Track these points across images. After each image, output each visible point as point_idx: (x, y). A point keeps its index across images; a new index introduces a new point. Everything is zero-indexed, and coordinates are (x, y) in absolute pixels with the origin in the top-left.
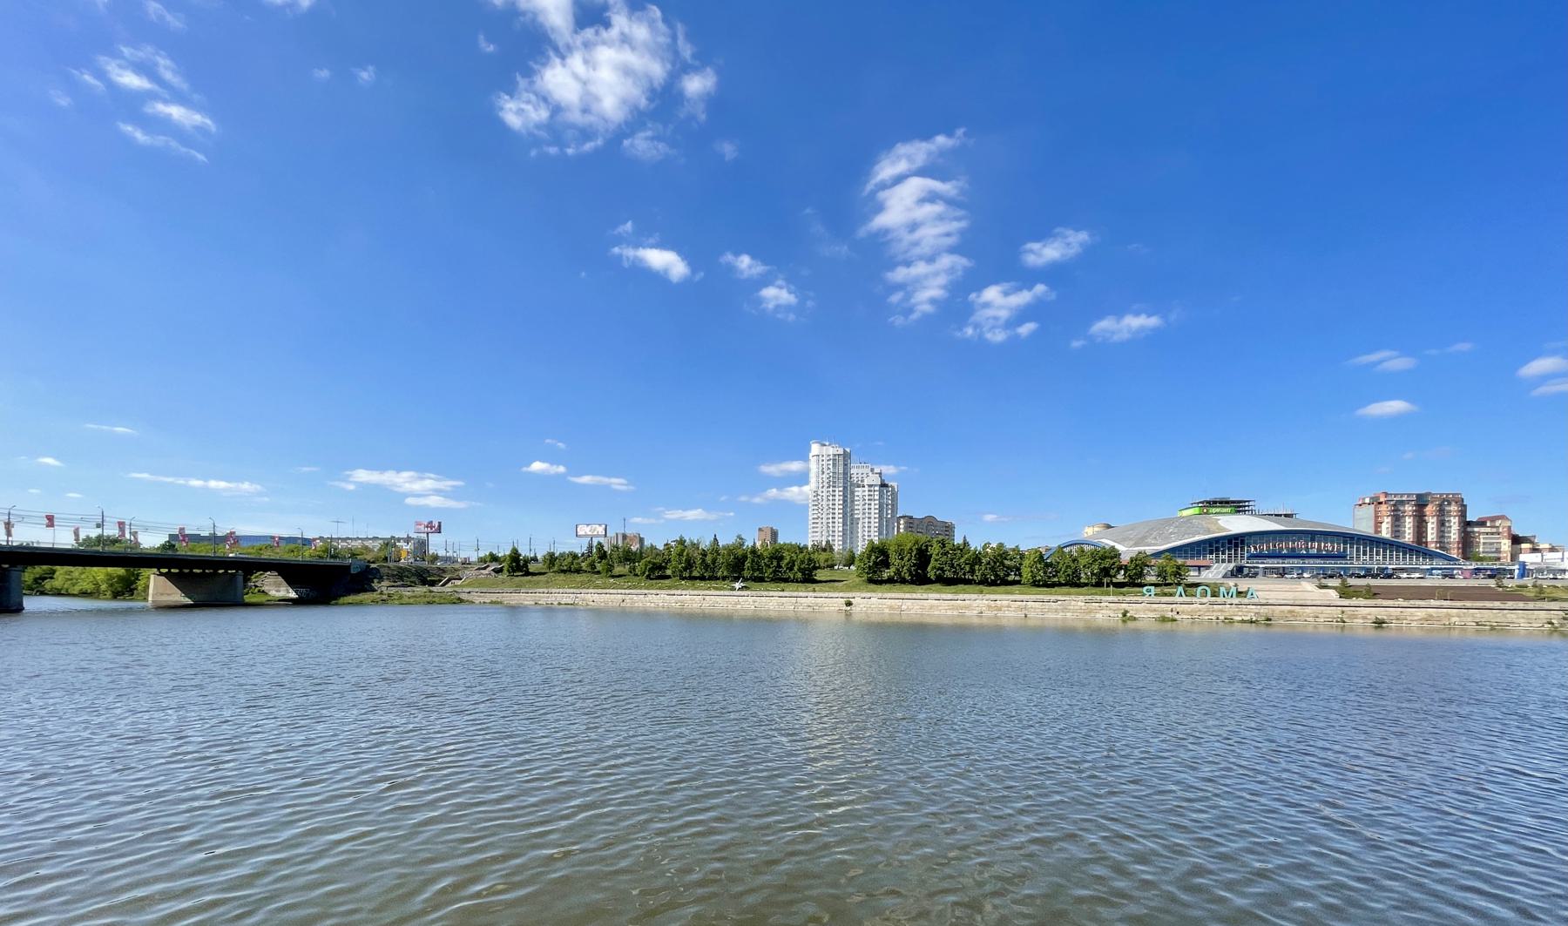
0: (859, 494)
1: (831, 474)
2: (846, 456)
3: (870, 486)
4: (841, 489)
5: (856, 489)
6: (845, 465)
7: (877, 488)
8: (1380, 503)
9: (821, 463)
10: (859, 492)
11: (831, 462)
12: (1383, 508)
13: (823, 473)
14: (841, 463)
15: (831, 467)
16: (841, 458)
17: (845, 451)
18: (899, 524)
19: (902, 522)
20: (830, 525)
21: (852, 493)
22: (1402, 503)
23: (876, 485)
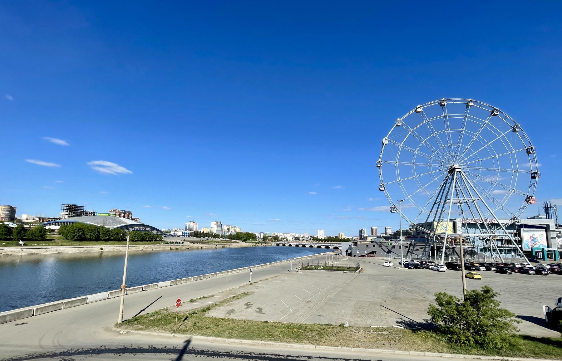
8: (117, 212)
12: (117, 213)
22: (121, 213)
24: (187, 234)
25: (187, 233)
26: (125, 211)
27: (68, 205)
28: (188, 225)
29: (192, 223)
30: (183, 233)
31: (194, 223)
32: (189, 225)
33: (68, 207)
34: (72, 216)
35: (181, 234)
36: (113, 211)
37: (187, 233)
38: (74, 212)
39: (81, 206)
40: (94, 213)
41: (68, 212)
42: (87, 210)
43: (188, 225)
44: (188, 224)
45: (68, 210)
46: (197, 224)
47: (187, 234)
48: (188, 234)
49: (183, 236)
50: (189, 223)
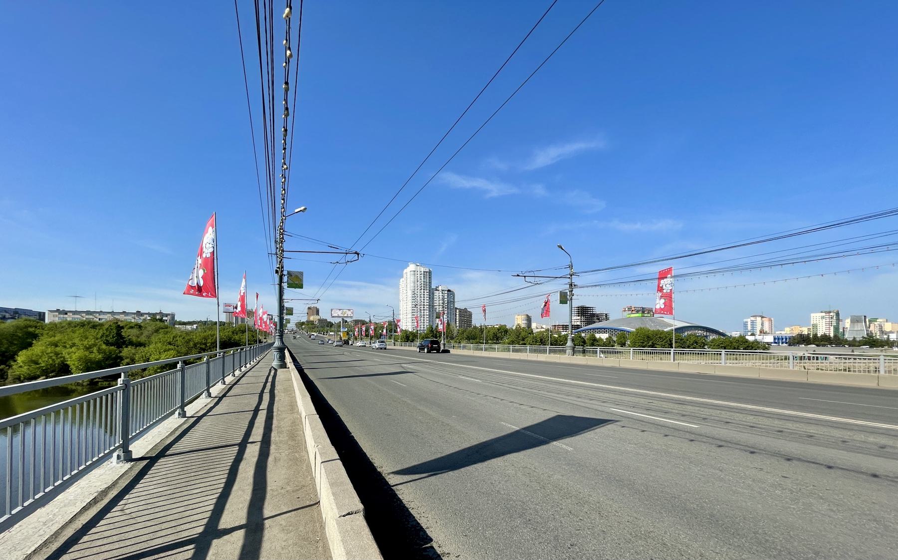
0: (437, 294)
1: (422, 282)
2: (430, 272)
3: (443, 290)
4: (428, 291)
5: (435, 292)
6: (430, 278)
7: (446, 292)
9: (416, 276)
10: (436, 293)
11: (422, 275)
13: (418, 281)
14: (428, 276)
15: (422, 278)
16: (428, 274)
17: (429, 270)
18: (456, 311)
19: (458, 311)
20: (422, 311)
21: (433, 294)
23: (445, 291)
24: (784, 340)
25: (779, 339)
26: (643, 308)
27: (578, 308)
28: (749, 324)
29: (759, 319)
30: (775, 339)
31: (764, 319)
32: (753, 322)
33: (578, 310)
34: (584, 320)
35: (772, 340)
36: (627, 309)
37: (782, 339)
38: (585, 316)
39: (590, 307)
40: (606, 314)
41: (579, 316)
42: (597, 311)
43: (749, 324)
44: (749, 320)
45: (578, 314)
46: (772, 319)
47: (784, 340)
48: (786, 339)
49: (776, 343)
50: (752, 319)
